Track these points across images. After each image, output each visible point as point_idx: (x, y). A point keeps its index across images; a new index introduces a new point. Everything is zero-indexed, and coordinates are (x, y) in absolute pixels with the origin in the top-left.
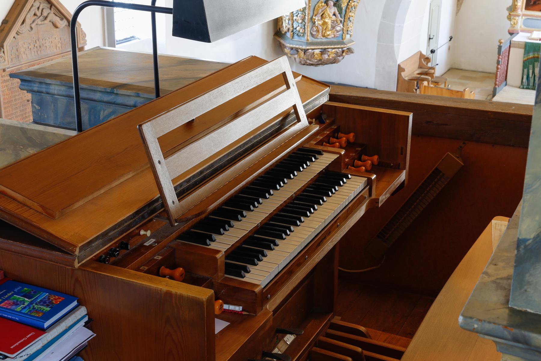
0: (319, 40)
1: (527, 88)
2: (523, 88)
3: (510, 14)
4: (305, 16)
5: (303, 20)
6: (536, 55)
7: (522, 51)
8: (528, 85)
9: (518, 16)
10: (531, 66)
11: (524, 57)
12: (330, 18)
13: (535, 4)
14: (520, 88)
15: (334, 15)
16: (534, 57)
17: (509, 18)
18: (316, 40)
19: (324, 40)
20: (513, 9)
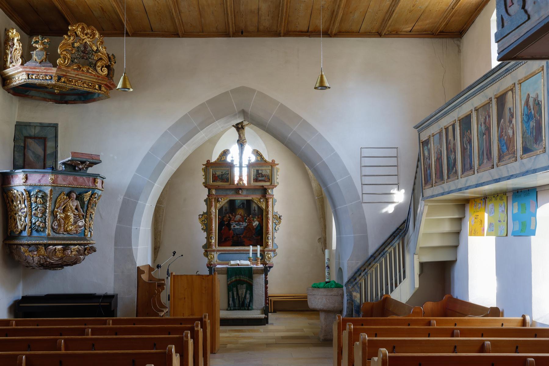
0: (61, 236)
1: (234, 310)
2: (231, 310)
3: (206, 251)
6: (238, 278)
7: (224, 277)
8: (235, 306)
9: (214, 251)
10: (235, 289)
11: (228, 281)
12: (73, 211)
14: (227, 310)
15: (76, 209)
16: (236, 280)
17: (206, 254)
19: (66, 236)
20: (207, 247)
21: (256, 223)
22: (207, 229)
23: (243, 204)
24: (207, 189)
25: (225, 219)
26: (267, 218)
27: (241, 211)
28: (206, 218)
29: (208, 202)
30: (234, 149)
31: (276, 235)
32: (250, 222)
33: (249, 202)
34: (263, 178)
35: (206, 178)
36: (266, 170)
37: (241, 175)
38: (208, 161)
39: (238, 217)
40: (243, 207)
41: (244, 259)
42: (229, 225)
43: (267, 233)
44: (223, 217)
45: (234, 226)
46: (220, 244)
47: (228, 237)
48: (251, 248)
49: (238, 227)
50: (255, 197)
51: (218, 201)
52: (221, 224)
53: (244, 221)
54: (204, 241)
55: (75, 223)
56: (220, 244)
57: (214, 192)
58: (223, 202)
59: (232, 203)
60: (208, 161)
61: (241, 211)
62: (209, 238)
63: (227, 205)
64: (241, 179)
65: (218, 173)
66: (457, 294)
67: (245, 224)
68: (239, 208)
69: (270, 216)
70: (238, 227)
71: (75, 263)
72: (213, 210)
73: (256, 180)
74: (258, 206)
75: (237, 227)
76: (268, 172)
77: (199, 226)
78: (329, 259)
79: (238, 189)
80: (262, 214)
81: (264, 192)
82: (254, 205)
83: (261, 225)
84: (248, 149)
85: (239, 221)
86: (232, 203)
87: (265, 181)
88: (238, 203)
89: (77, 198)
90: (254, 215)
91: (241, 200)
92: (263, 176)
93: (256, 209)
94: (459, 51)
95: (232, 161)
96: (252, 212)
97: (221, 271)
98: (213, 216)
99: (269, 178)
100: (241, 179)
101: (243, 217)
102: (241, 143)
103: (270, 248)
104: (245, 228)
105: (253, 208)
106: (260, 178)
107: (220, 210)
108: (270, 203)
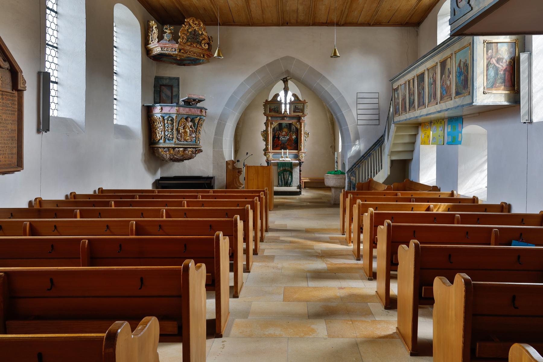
3: (265, 153)
7: (276, 167)
9: (270, 152)
12: (189, 129)
13: (276, 146)
15: (191, 127)
17: (265, 155)
20: (266, 150)
21: (294, 137)
22: (266, 140)
23: (287, 125)
24: (266, 117)
26: (301, 134)
28: (265, 134)
29: (266, 124)
30: (282, 94)
31: (306, 144)
32: (291, 136)
33: (290, 125)
35: (265, 110)
36: (300, 106)
37: (286, 109)
38: (267, 101)
39: (284, 133)
41: (287, 156)
42: (278, 138)
45: (282, 138)
47: (278, 145)
51: (272, 124)
52: (274, 137)
53: (287, 135)
54: (264, 147)
55: (190, 135)
57: (270, 118)
58: (275, 124)
59: (280, 125)
60: (267, 101)
61: (286, 130)
62: (267, 145)
64: (285, 111)
65: (272, 107)
67: (288, 137)
69: (303, 133)
71: (191, 158)
72: (269, 128)
73: (294, 112)
77: (261, 138)
78: (337, 158)
79: (284, 117)
80: (298, 132)
81: (299, 119)
82: (293, 127)
83: (297, 138)
84: (290, 94)
85: (285, 135)
86: (280, 125)
87: (299, 112)
88: (284, 125)
89: (191, 121)
90: (293, 132)
95: (281, 100)
96: (292, 130)
97: (274, 164)
98: (269, 132)
99: (302, 111)
100: (285, 111)
101: (286, 133)
102: (286, 90)
103: (303, 151)
104: (288, 139)
107: (274, 129)
108: (303, 125)
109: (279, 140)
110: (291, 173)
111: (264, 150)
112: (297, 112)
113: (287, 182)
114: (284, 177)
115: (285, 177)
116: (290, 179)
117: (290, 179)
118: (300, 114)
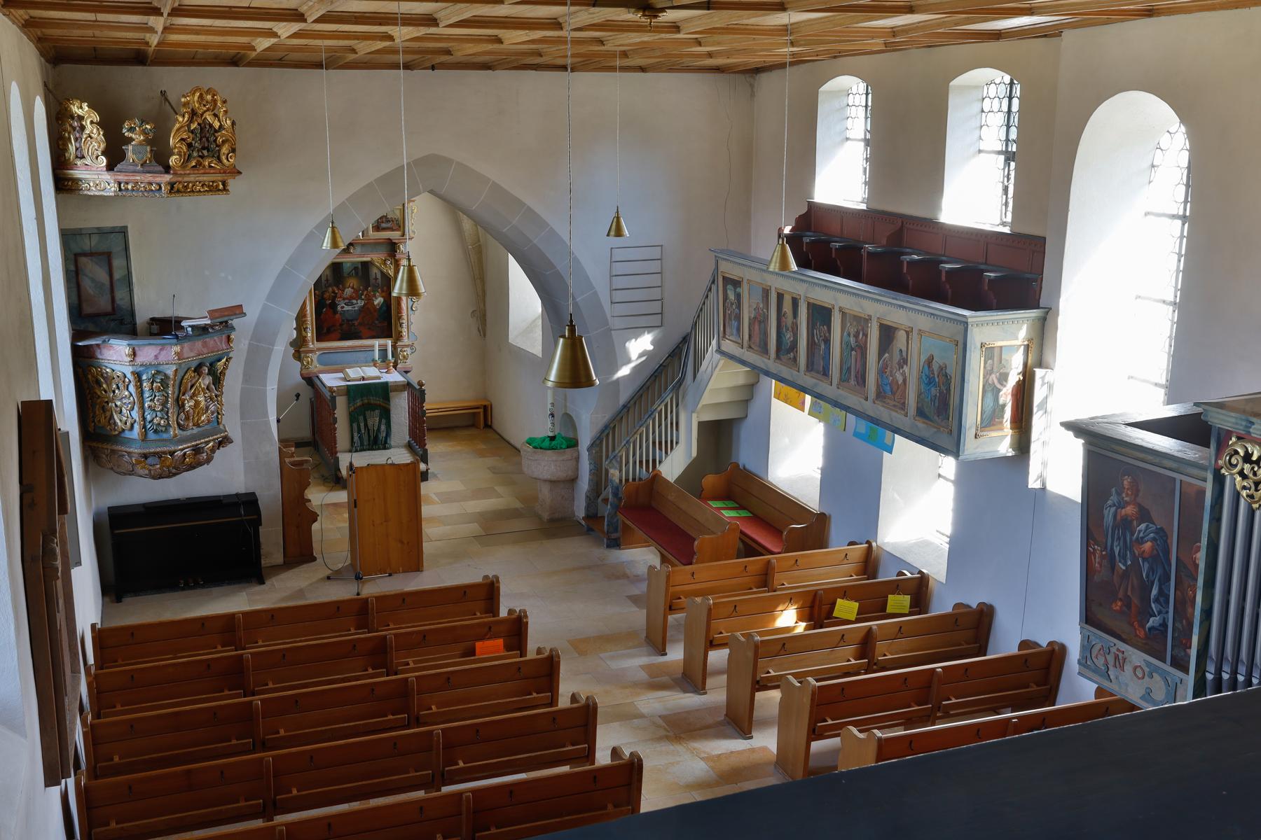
4: (167, 397)
5: (164, 404)
13: (329, 331)
18: (188, 433)
21: (379, 301)
23: (356, 268)
25: (327, 295)
27: (353, 282)
32: (369, 300)
33: (366, 265)
34: (389, 225)
39: (348, 291)
40: (357, 274)
42: (333, 306)
43: (400, 318)
44: (323, 293)
45: (342, 306)
46: (320, 337)
48: (377, 343)
49: (349, 308)
50: (376, 257)
56: (320, 337)
61: (353, 282)
63: (328, 272)
66: (745, 457)
67: (361, 303)
68: (350, 275)
70: (349, 308)
73: (377, 228)
74: (382, 273)
75: (347, 308)
76: (398, 214)
81: (392, 247)
82: (374, 271)
85: (351, 298)
87: (391, 229)
90: (376, 287)
91: (353, 263)
92: (388, 221)
93: (379, 276)
94: (753, 95)
96: (372, 281)
101: (356, 291)
104: (362, 309)
105: (372, 276)
106: (384, 225)
109: (335, 312)
110: (386, 414)
111: (292, 344)
112: (384, 229)
113: (376, 438)
114: (366, 425)
115: (370, 423)
116: (383, 427)
117: (383, 427)
118: (394, 235)
